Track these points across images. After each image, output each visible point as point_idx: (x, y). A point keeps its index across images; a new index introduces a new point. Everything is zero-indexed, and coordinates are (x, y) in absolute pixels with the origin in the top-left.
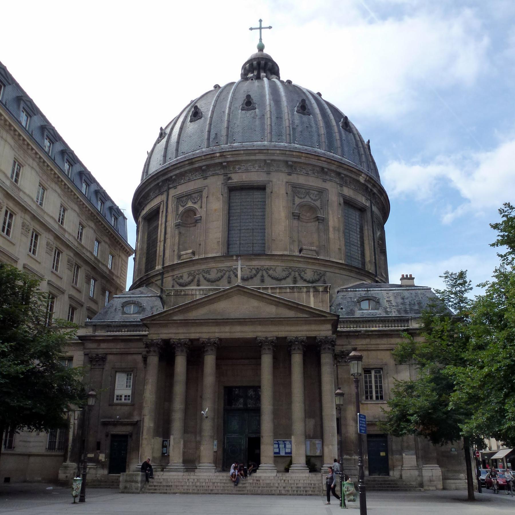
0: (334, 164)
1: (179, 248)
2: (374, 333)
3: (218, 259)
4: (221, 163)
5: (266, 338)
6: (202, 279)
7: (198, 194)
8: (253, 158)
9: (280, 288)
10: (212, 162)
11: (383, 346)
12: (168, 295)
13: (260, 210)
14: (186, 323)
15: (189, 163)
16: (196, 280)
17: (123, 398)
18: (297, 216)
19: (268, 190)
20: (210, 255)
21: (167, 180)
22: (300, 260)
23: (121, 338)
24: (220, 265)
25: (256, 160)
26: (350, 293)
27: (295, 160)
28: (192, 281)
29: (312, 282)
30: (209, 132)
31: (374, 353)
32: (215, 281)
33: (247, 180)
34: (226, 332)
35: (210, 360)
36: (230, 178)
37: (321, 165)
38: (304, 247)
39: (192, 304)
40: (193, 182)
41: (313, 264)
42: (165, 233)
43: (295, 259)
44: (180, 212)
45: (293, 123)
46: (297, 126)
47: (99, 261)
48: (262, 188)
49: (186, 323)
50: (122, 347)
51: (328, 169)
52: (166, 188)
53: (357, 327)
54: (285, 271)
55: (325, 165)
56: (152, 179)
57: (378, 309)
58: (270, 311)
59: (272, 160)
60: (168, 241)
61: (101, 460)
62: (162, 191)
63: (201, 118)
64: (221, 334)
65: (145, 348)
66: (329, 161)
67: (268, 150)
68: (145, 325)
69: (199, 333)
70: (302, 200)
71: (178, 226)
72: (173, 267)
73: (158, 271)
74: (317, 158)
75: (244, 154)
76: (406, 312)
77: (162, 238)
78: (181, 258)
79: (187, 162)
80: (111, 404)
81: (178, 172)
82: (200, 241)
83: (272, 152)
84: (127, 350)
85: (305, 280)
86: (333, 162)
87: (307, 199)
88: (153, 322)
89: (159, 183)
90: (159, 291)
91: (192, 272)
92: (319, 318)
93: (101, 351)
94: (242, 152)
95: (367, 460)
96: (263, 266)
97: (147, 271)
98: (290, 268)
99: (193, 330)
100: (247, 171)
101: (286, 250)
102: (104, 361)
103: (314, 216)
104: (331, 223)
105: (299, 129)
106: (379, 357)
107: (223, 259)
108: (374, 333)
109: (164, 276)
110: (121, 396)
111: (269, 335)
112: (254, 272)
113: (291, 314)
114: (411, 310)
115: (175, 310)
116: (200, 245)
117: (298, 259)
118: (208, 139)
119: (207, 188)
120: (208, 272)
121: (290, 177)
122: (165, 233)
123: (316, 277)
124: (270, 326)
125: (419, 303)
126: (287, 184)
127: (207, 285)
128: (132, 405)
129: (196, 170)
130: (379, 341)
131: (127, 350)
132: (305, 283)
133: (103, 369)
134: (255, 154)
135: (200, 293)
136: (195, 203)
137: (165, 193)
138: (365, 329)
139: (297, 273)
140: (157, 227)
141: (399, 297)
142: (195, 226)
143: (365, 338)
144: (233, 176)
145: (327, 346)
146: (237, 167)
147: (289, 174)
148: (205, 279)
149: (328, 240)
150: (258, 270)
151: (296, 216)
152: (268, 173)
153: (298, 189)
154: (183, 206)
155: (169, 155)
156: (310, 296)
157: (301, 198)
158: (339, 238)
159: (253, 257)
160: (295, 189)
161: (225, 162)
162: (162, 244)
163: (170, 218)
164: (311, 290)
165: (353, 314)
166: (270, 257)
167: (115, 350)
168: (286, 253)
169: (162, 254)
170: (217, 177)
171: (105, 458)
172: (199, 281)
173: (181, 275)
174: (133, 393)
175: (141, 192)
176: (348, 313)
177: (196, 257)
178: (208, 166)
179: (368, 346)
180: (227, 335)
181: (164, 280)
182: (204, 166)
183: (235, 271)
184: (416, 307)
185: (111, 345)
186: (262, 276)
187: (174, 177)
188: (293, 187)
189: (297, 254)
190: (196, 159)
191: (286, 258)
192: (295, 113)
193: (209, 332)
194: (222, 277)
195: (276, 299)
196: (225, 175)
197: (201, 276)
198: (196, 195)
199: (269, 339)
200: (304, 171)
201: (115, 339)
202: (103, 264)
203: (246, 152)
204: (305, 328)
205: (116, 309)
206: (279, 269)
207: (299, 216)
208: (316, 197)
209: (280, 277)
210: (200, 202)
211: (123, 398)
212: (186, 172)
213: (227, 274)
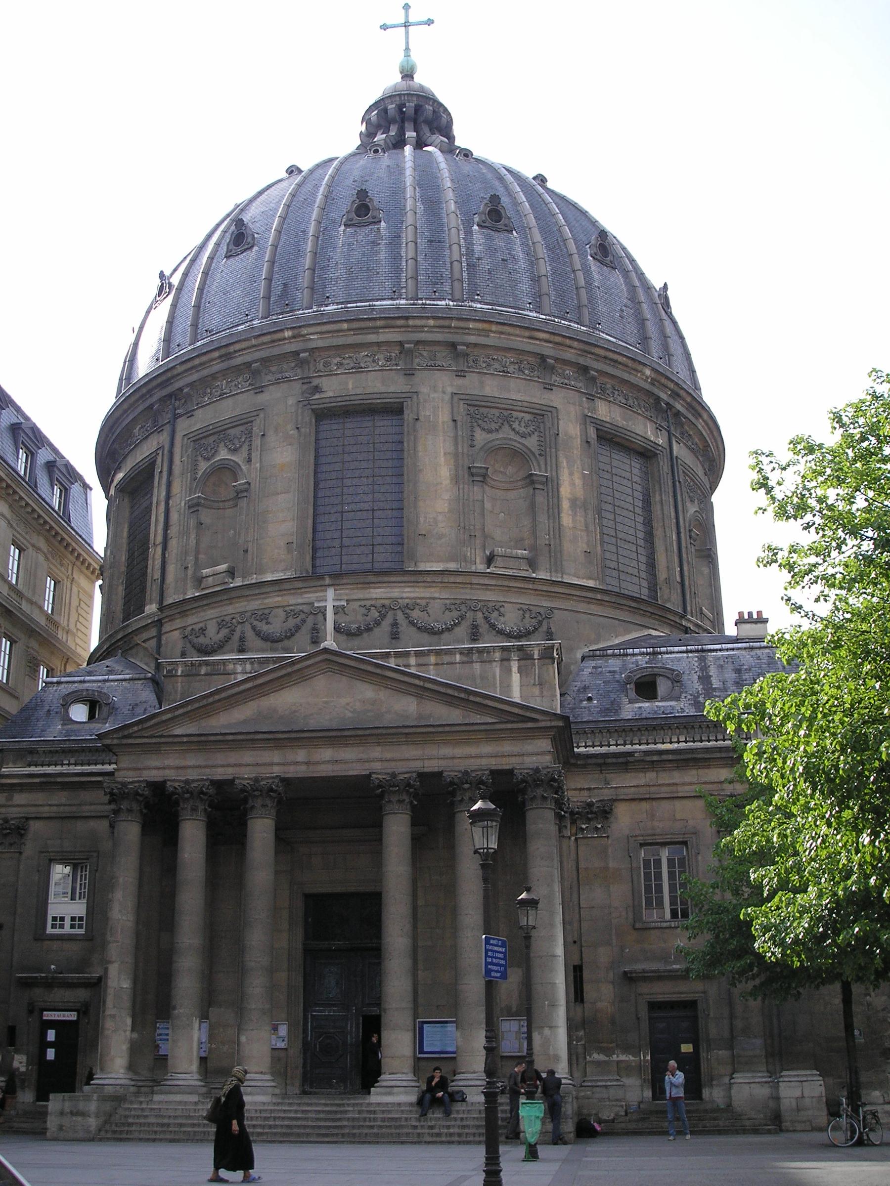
1: (197, 559)
2: (665, 757)
4: (297, 353)
5: (394, 775)
8: (372, 338)
9: (438, 653)
10: (276, 351)
11: (687, 788)
12: (171, 675)
13: (390, 464)
14: (204, 743)
15: (220, 357)
17: (67, 922)
18: (478, 475)
19: (408, 415)
20: (269, 577)
22: (486, 581)
23: (59, 780)
24: (292, 600)
25: (378, 344)
26: (611, 661)
27: (472, 339)
28: (228, 639)
29: (519, 637)
30: (269, 280)
31: (666, 805)
32: (281, 640)
33: (359, 391)
34: (296, 763)
35: (261, 830)
37: (537, 350)
38: (499, 550)
39: (217, 697)
40: (230, 401)
41: (521, 591)
43: (475, 580)
44: (200, 473)
45: (470, 252)
46: (479, 259)
47: (19, 594)
49: (204, 743)
50: (64, 801)
51: (557, 360)
52: (167, 417)
53: (624, 745)
54: (450, 610)
55: (547, 350)
56: (137, 396)
57: (678, 699)
58: (405, 708)
59: (418, 343)
60: (173, 544)
61: (18, 1069)
63: (252, 246)
64: (286, 768)
65: (110, 803)
66: (558, 339)
68: (108, 748)
69: (235, 765)
70: (493, 436)
71: (194, 507)
72: (184, 607)
73: (149, 616)
74: (527, 334)
75: (349, 330)
77: (160, 539)
78: (202, 586)
79: (216, 354)
80: (40, 936)
81: (195, 377)
83: (418, 322)
84: (74, 809)
85: (501, 632)
86: (568, 342)
87: (506, 433)
88: (125, 741)
89: (151, 407)
90: (153, 665)
91: (227, 619)
92: (520, 725)
93: (14, 812)
94: (345, 326)
95: (648, 1064)
96: (395, 600)
97: (127, 616)
98: (464, 602)
99: (220, 758)
100: (358, 369)
101: (452, 559)
102: (22, 835)
103: (522, 474)
104: (565, 491)
105: (485, 265)
106: (678, 816)
107: (300, 584)
108: (665, 757)
109: (164, 630)
110: (62, 919)
111: (399, 768)
112: (375, 614)
113: (455, 715)
115: (177, 713)
116: (246, 551)
117: (481, 582)
118: (267, 297)
119: (262, 415)
121: (460, 381)
123: (529, 624)
124: (404, 747)
126: (456, 398)
127: (263, 650)
128: (89, 938)
129: (238, 370)
130: (677, 777)
131: (74, 809)
132: (501, 637)
133: (21, 853)
134: (375, 330)
136: (235, 451)
137: (168, 428)
138: (643, 747)
139: (480, 614)
140: (148, 510)
141: (730, 667)
142: (236, 506)
143: (644, 770)
145: (540, 792)
147: (461, 374)
148: (258, 633)
150: (384, 610)
152: (409, 373)
153: (482, 410)
154: (208, 459)
155: (178, 339)
156: (509, 671)
157: (490, 431)
158: (587, 526)
159: (372, 578)
160: (475, 411)
161: (304, 351)
162: (159, 550)
163: (176, 488)
164: (514, 657)
165: (617, 712)
166: (413, 579)
167: (47, 809)
168: (452, 566)
169: (157, 575)
170: (285, 386)
171: (27, 1066)
172: (242, 639)
173: (201, 625)
174: (90, 910)
175: (112, 427)
176: (605, 711)
177: (238, 582)
178: (265, 361)
179: (653, 789)
180: (301, 771)
181: (164, 638)
182: (256, 361)
185: (39, 797)
186: (395, 624)
189: (481, 567)
190: (238, 347)
191: (452, 579)
192: (476, 227)
194: (298, 628)
195: (417, 682)
196: (306, 380)
197: (248, 628)
199: (401, 777)
200: (497, 365)
201: (47, 784)
202: (31, 602)
203: (355, 325)
205: (49, 711)
206: (436, 608)
207: (485, 476)
208: (526, 427)
209: (439, 626)
210: (245, 447)
211: (67, 922)
212: (214, 376)
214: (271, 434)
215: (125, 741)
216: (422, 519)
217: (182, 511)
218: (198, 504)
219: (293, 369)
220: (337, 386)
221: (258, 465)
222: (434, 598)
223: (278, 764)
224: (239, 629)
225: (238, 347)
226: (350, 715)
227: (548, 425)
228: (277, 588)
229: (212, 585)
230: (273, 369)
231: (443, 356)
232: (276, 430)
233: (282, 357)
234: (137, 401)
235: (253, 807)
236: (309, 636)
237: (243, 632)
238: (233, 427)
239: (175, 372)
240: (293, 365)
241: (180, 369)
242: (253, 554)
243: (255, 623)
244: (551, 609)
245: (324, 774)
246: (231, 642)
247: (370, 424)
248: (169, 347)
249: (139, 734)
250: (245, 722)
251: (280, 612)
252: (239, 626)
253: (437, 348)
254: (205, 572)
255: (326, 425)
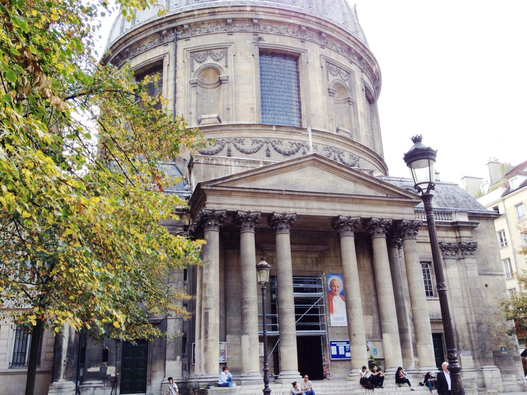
0: (359, 47)
3: (254, 128)
6: (233, 149)
7: (222, 50)
14: (256, 193)
15: (209, 13)
16: (225, 149)
19: (303, 59)
21: (174, 29)
24: (255, 135)
25: (290, 24)
32: (251, 153)
34: (302, 208)
36: (260, 39)
42: (175, 92)
43: (335, 138)
48: (295, 57)
49: (256, 193)
52: (171, 39)
56: (152, 25)
59: (307, 28)
62: (165, 41)
66: (356, 42)
67: (305, 15)
69: (272, 206)
70: (335, 78)
71: (194, 84)
74: (347, 36)
75: (279, 14)
76: (445, 205)
79: (207, 11)
81: (192, 20)
82: (228, 104)
86: (359, 44)
87: (338, 77)
88: (214, 188)
89: (162, 31)
91: (220, 140)
94: (277, 11)
100: (280, 34)
101: (325, 127)
103: (342, 98)
112: (295, 147)
114: (449, 203)
116: (228, 109)
119: (233, 45)
120: (241, 141)
121: (322, 50)
122: (175, 92)
125: (454, 198)
126: (322, 57)
129: (217, 22)
134: (290, 17)
135: (235, 164)
136: (218, 60)
139: (336, 154)
144: (264, 36)
146: (270, 27)
147: (323, 47)
148: (238, 149)
149: (358, 124)
151: (330, 93)
153: (330, 65)
154: (201, 62)
157: (334, 75)
160: (330, 65)
163: (180, 73)
170: (244, 34)
172: (229, 150)
178: (233, 20)
182: (229, 19)
183: (274, 143)
184: (453, 201)
187: (186, 27)
188: (326, 62)
190: (220, 10)
191: (327, 136)
193: (282, 207)
194: (259, 149)
196: (255, 34)
198: (218, 51)
200: (334, 47)
204: (388, 209)
210: (223, 60)
212: (203, 23)
213: (265, 146)
214: (238, 55)
215: (214, 188)
216: (312, 108)
217: (186, 85)
218: (196, 83)
219: (248, 27)
220: (271, 40)
221: (233, 69)
222: (319, 144)
223: (293, 208)
224: (227, 146)
225: (220, 10)
226: (323, 187)
227: (352, 78)
228: (248, 128)
229: (206, 123)
230: (237, 25)
231: (315, 37)
232: (241, 54)
233: (243, 20)
234: (149, 28)
235: (281, 229)
236: (265, 153)
237: (229, 147)
238: (215, 49)
239: (180, 16)
240: (247, 25)
241: (183, 15)
242: (233, 110)
243: (236, 143)
244: (359, 157)
245: (315, 215)
246: (222, 151)
247: (284, 61)
248: (169, 5)
249: (220, 185)
250: (273, 185)
251: (250, 139)
252: (227, 144)
253: (313, 33)
254: (203, 116)
255: (263, 58)
